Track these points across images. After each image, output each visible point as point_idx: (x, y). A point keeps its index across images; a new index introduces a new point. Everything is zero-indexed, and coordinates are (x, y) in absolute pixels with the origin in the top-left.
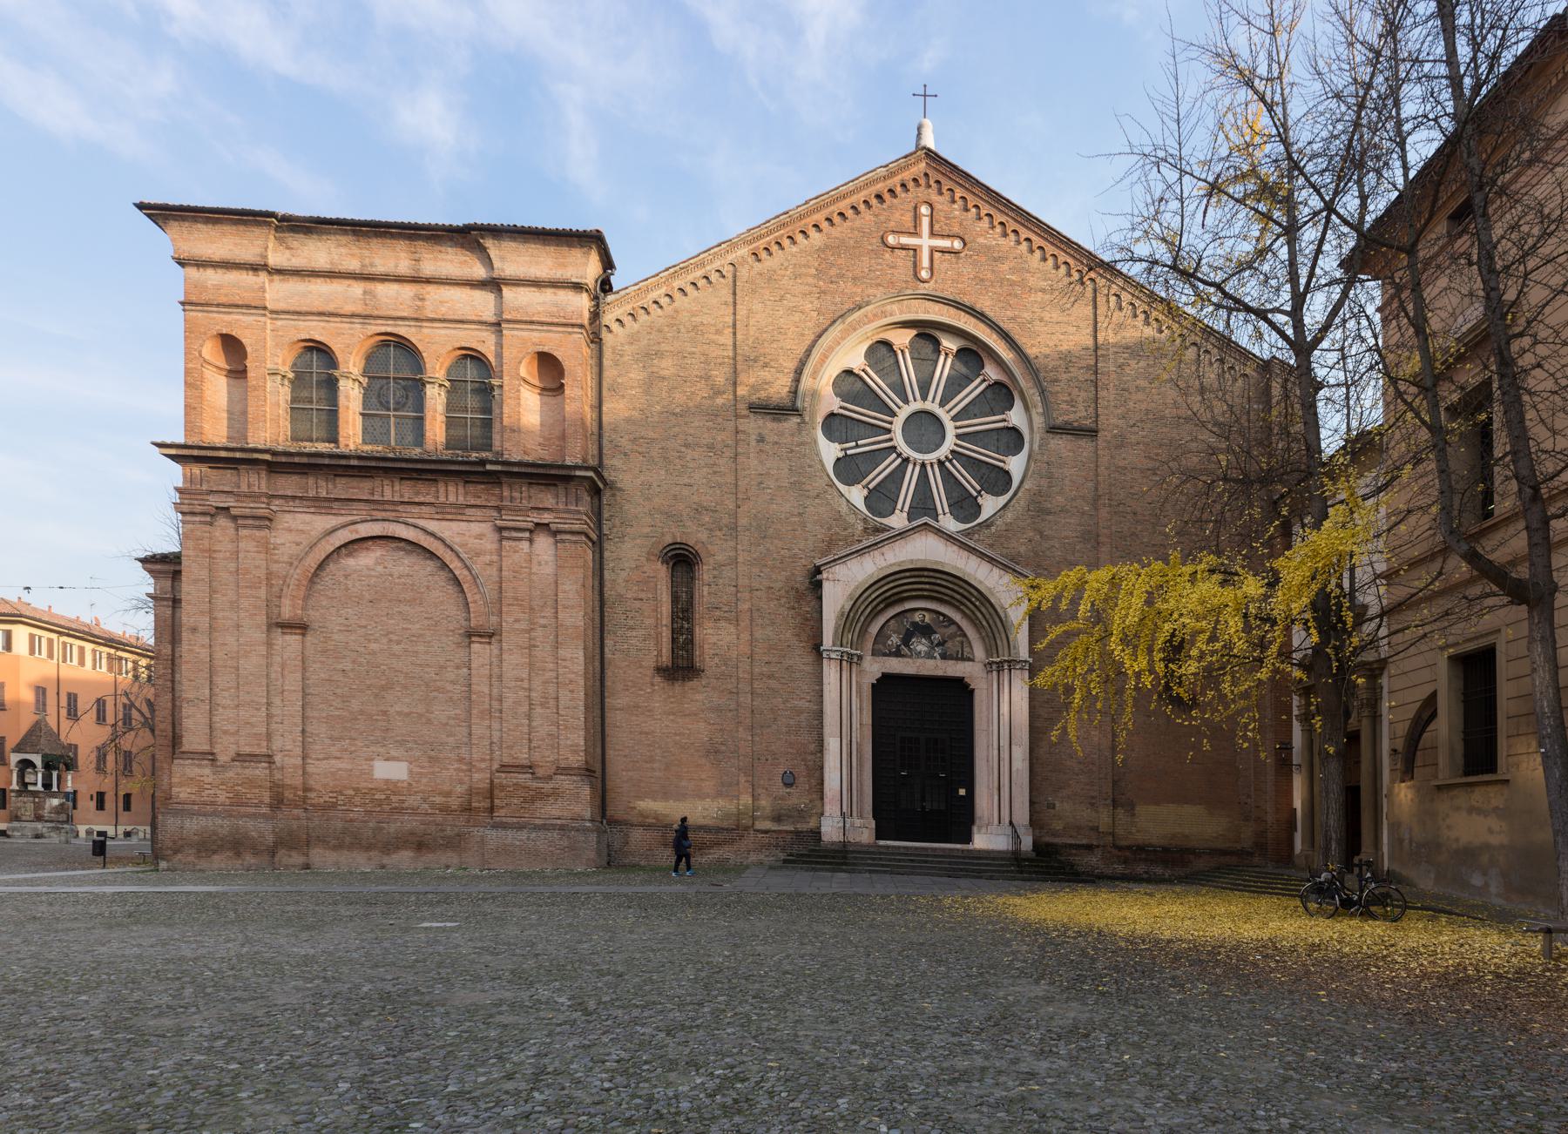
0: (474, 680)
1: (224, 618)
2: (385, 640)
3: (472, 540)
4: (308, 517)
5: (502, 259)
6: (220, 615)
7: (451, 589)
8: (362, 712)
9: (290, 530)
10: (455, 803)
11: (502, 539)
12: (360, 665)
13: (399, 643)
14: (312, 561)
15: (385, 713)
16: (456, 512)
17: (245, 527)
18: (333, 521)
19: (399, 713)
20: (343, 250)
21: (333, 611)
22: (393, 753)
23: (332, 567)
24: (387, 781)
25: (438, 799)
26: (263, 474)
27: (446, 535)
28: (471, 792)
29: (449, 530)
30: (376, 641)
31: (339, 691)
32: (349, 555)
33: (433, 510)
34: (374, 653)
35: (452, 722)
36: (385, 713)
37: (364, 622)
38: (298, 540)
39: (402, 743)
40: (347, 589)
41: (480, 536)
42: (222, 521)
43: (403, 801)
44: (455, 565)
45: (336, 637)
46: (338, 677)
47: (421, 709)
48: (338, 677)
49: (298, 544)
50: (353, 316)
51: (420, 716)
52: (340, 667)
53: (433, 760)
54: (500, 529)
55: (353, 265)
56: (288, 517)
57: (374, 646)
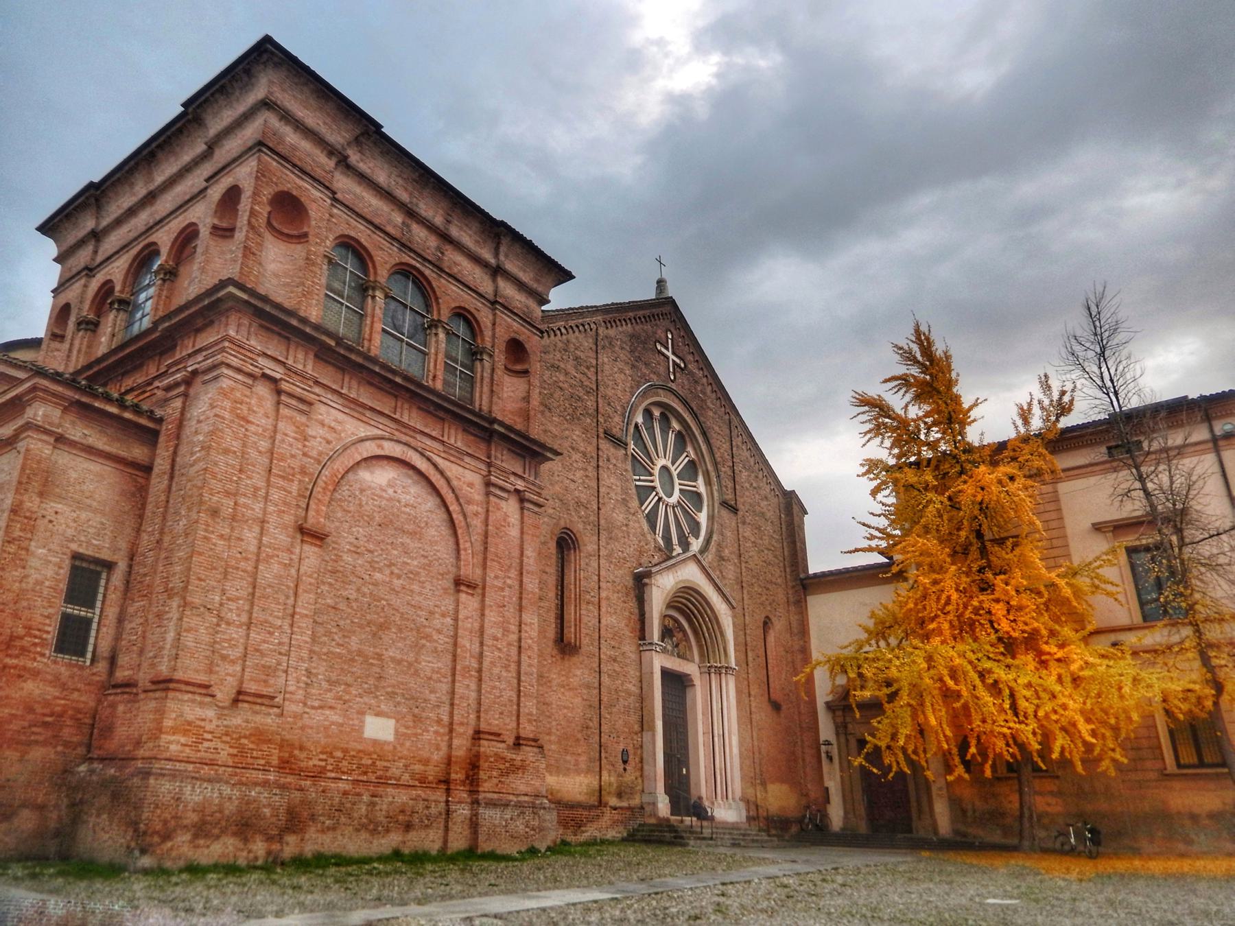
0: (460, 631)
1: (246, 506)
2: (387, 572)
3: (465, 487)
4: (340, 416)
5: (506, 256)
6: (242, 500)
7: (445, 531)
8: (360, 653)
9: (323, 425)
10: (432, 772)
11: (488, 494)
12: (364, 595)
13: (399, 577)
14: (340, 465)
15: (379, 657)
16: (458, 455)
17: (287, 406)
18: (364, 431)
19: (393, 659)
21: (346, 526)
23: (351, 476)
24: (375, 742)
25: (418, 768)
26: (311, 356)
27: (449, 474)
28: (449, 761)
29: (452, 470)
30: (380, 570)
31: (342, 623)
32: (368, 468)
33: (441, 448)
34: (376, 584)
35: (435, 676)
37: (371, 547)
38: (329, 436)
39: (392, 695)
40: (360, 505)
41: (471, 485)
42: (263, 390)
43: (387, 769)
44: (454, 507)
45: (345, 557)
46: (342, 606)
47: (411, 657)
48: (342, 606)
49: (328, 442)
51: (410, 665)
52: (345, 593)
53: (417, 719)
54: (488, 484)
56: (323, 408)
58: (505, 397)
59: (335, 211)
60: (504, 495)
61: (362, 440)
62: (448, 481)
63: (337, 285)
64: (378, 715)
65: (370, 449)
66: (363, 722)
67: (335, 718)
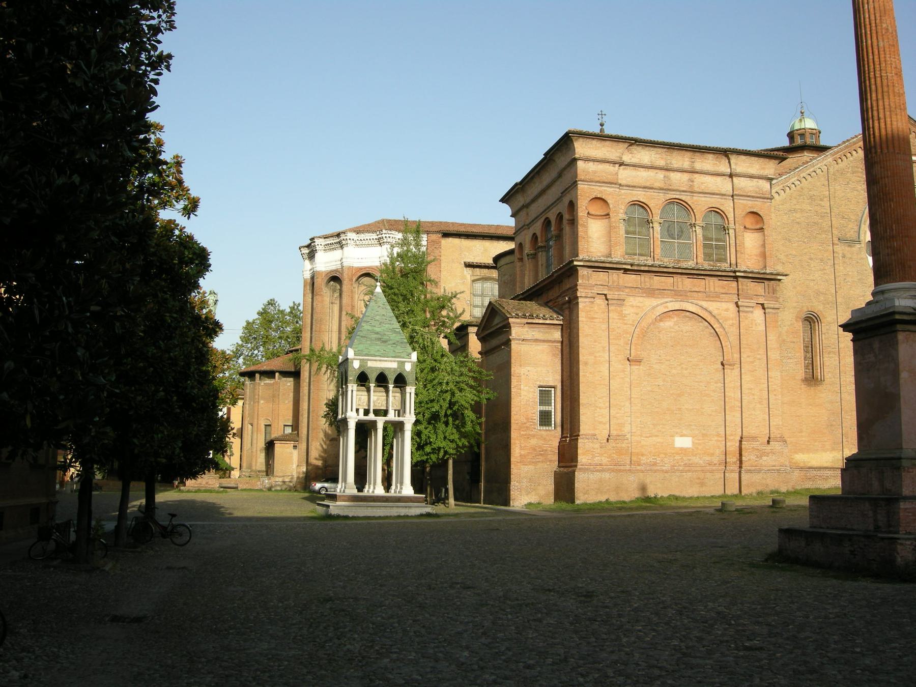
4: (641, 299)
9: (632, 306)
13: (686, 369)
15: (680, 409)
18: (654, 302)
20: (658, 156)
22: (684, 432)
24: (681, 449)
27: (710, 309)
29: (713, 306)
32: (661, 320)
36: (680, 409)
37: (668, 358)
41: (727, 310)
43: (689, 460)
50: (661, 189)
55: (662, 163)
56: (632, 299)
57: (674, 371)
58: (747, 250)
59: (623, 191)
60: (751, 309)
61: (657, 306)
62: (710, 313)
63: (631, 229)
64: (681, 436)
65: (661, 310)
66: (674, 441)
67: (659, 440)
